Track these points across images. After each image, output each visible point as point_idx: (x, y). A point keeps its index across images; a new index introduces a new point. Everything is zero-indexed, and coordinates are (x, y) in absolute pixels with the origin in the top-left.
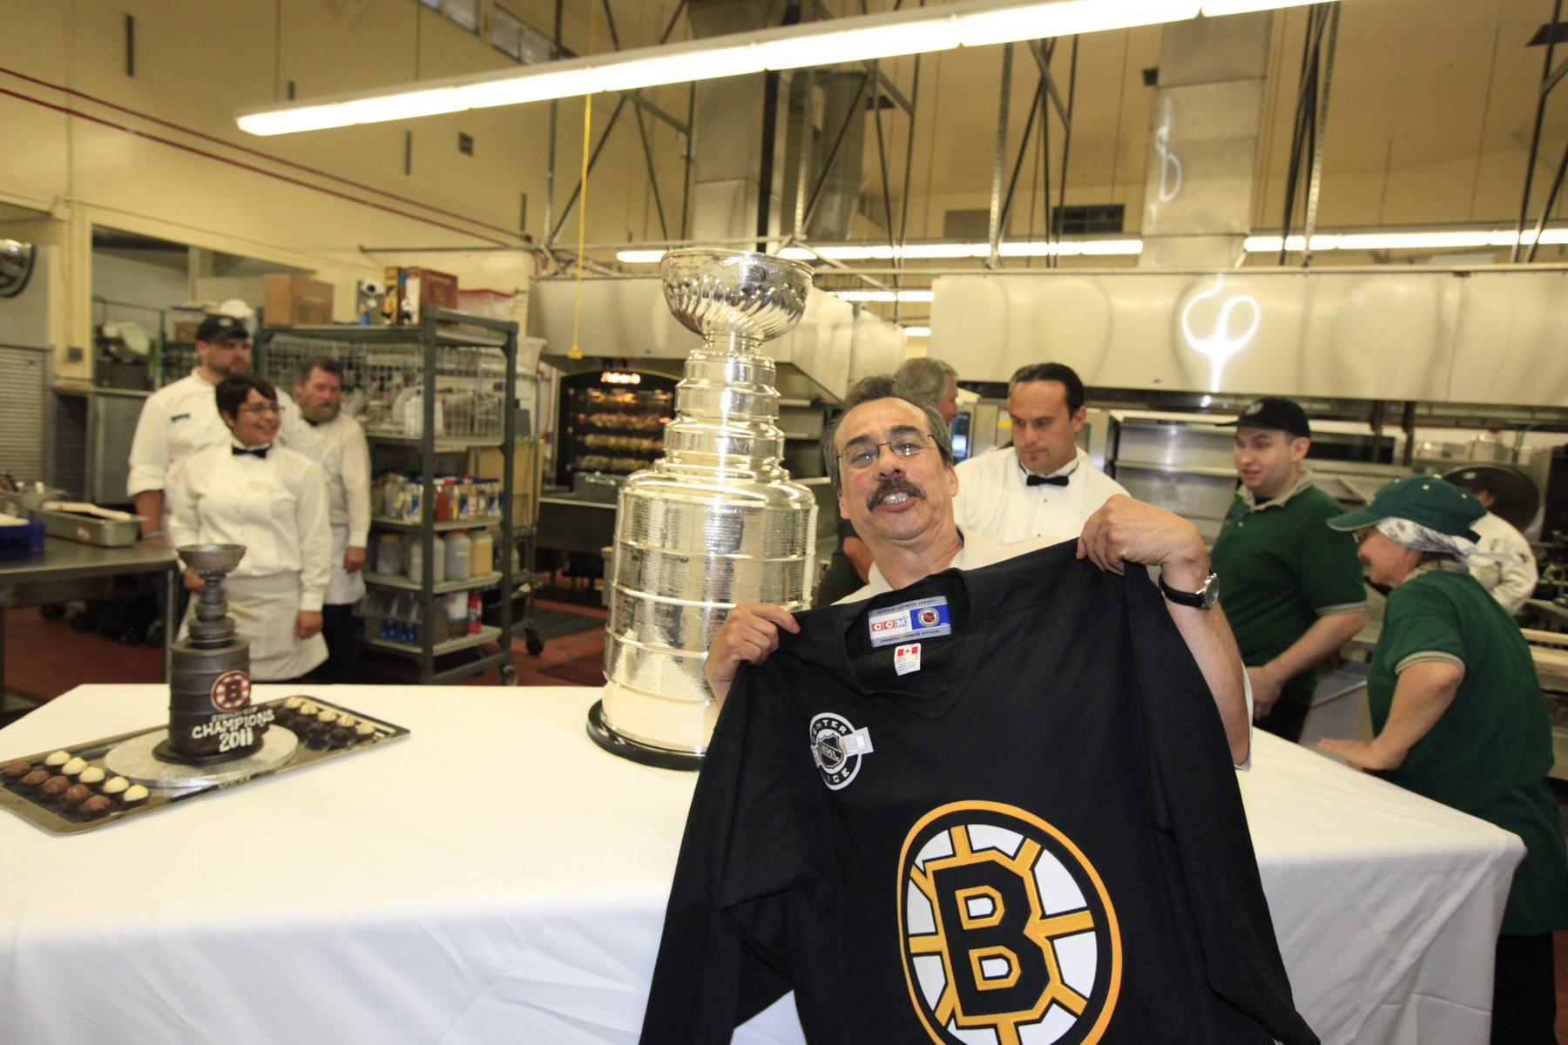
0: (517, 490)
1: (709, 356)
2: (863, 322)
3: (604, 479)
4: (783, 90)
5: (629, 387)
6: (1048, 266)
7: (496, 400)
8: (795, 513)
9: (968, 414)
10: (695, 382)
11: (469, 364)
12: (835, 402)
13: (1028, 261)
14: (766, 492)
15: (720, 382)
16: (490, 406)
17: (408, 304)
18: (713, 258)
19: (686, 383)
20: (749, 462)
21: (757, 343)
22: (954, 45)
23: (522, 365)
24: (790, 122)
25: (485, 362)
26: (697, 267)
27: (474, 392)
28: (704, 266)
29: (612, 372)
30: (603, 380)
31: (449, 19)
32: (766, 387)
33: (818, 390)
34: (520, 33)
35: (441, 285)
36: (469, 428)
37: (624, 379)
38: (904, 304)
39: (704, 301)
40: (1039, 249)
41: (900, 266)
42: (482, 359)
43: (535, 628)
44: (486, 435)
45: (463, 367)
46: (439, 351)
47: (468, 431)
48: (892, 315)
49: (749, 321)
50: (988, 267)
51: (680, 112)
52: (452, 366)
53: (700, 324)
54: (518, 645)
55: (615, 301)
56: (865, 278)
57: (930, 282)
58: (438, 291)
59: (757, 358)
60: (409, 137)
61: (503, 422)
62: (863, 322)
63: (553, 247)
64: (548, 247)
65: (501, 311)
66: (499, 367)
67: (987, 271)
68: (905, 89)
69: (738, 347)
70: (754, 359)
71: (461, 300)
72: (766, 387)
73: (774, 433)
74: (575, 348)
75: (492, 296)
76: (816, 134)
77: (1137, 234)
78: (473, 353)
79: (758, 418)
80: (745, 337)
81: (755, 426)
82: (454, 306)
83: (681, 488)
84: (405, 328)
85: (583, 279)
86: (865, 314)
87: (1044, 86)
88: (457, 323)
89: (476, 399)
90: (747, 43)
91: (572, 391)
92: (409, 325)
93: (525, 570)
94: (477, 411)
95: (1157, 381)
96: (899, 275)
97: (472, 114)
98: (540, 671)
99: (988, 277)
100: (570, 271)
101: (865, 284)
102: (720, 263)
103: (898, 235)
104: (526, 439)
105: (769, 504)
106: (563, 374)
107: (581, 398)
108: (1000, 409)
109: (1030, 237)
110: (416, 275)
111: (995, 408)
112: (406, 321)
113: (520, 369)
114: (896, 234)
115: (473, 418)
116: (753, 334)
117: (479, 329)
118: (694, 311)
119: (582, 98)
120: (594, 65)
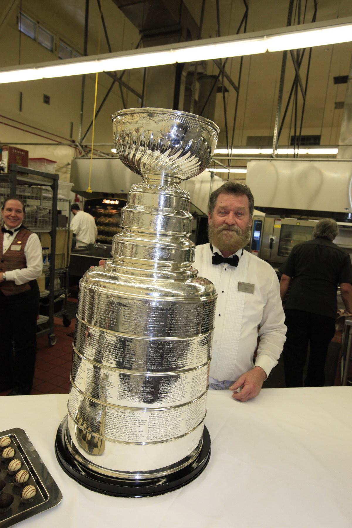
0: (57, 252)
1: (145, 189)
2: (215, 180)
3: (102, 246)
4: (183, 79)
5: (114, 206)
6: (294, 157)
7: (48, 211)
8: (204, 304)
9: (261, 221)
10: (135, 208)
11: (37, 194)
12: (202, 214)
13: (287, 156)
14: (184, 290)
15: (152, 208)
16: (46, 213)
17: (2, 163)
18: (148, 115)
19: (128, 208)
20: (170, 265)
21: (178, 181)
22: (264, 51)
23: (63, 195)
24: (185, 96)
25: (45, 193)
26: (136, 122)
27: (37, 207)
28: (142, 122)
29: (107, 199)
30: (103, 202)
31: (40, 44)
32: (184, 212)
33: (194, 209)
34: (71, 52)
35: (20, 155)
36: (34, 223)
37: (112, 202)
38: (232, 174)
39: (141, 148)
40: (291, 151)
41: (231, 156)
42: (43, 191)
43: (68, 314)
44: (43, 227)
45: (35, 195)
46: (19, 186)
47: (34, 226)
48: (226, 178)
49: (173, 164)
50: (272, 157)
51: (139, 89)
52: (29, 194)
53: (139, 165)
54: (58, 321)
55: (109, 168)
56: (216, 161)
57: (247, 164)
58: (18, 158)
59: (179, 191)
60: (21, 94)
61: (51, 221)
62: (215, 180)
63: (82, 144)
64: (80, 144)
65: (51, 169)
66: (51, 195)
67: (272, 159)
68: (236, 81)
69: (166, 182)
70: (176, 192)
71: (30, 162)
72: (184, 212)
73: (188, 244)
74: (89, 188)
75: (45, 161)
76: (196, 102)
77: (336, 146)
78: (38, 187)
79: (179, 234)
80: (170, 176)
81: (175, 239)
82: (27, 166)
83: (121, 285)
84: (1, 175)
85: (93, 158)
86: (216, 177)
87: (297, 80)
88: (27, 174)
89: (38, 211)
90: (168, 50)
91: (89, 207)
92: (3, 174)
93: (63, 288)
94: (39, 215)
95: (347, 209)
96: (230, 159)
97: (45, 81)
98: (68, 335)
99: (272, 161)
100: (89, 155)
101: (216, 164)
102: (154, 118)
103: (231, 145)
104: (64, 228)
105: (186, 298)
106: (86, 199)
107: (94, 210)
108: (275, 220)
109: (288, 147)
110: (7, 150)
111: (273, 219)
112: (2, 172)
113: (60, 196)
114: (229, 144)
115: (36, 219)
116: (177, 174)
117: (40, 177)
118: (134, 155)
119: (95, 74)
120: (99, 59)
